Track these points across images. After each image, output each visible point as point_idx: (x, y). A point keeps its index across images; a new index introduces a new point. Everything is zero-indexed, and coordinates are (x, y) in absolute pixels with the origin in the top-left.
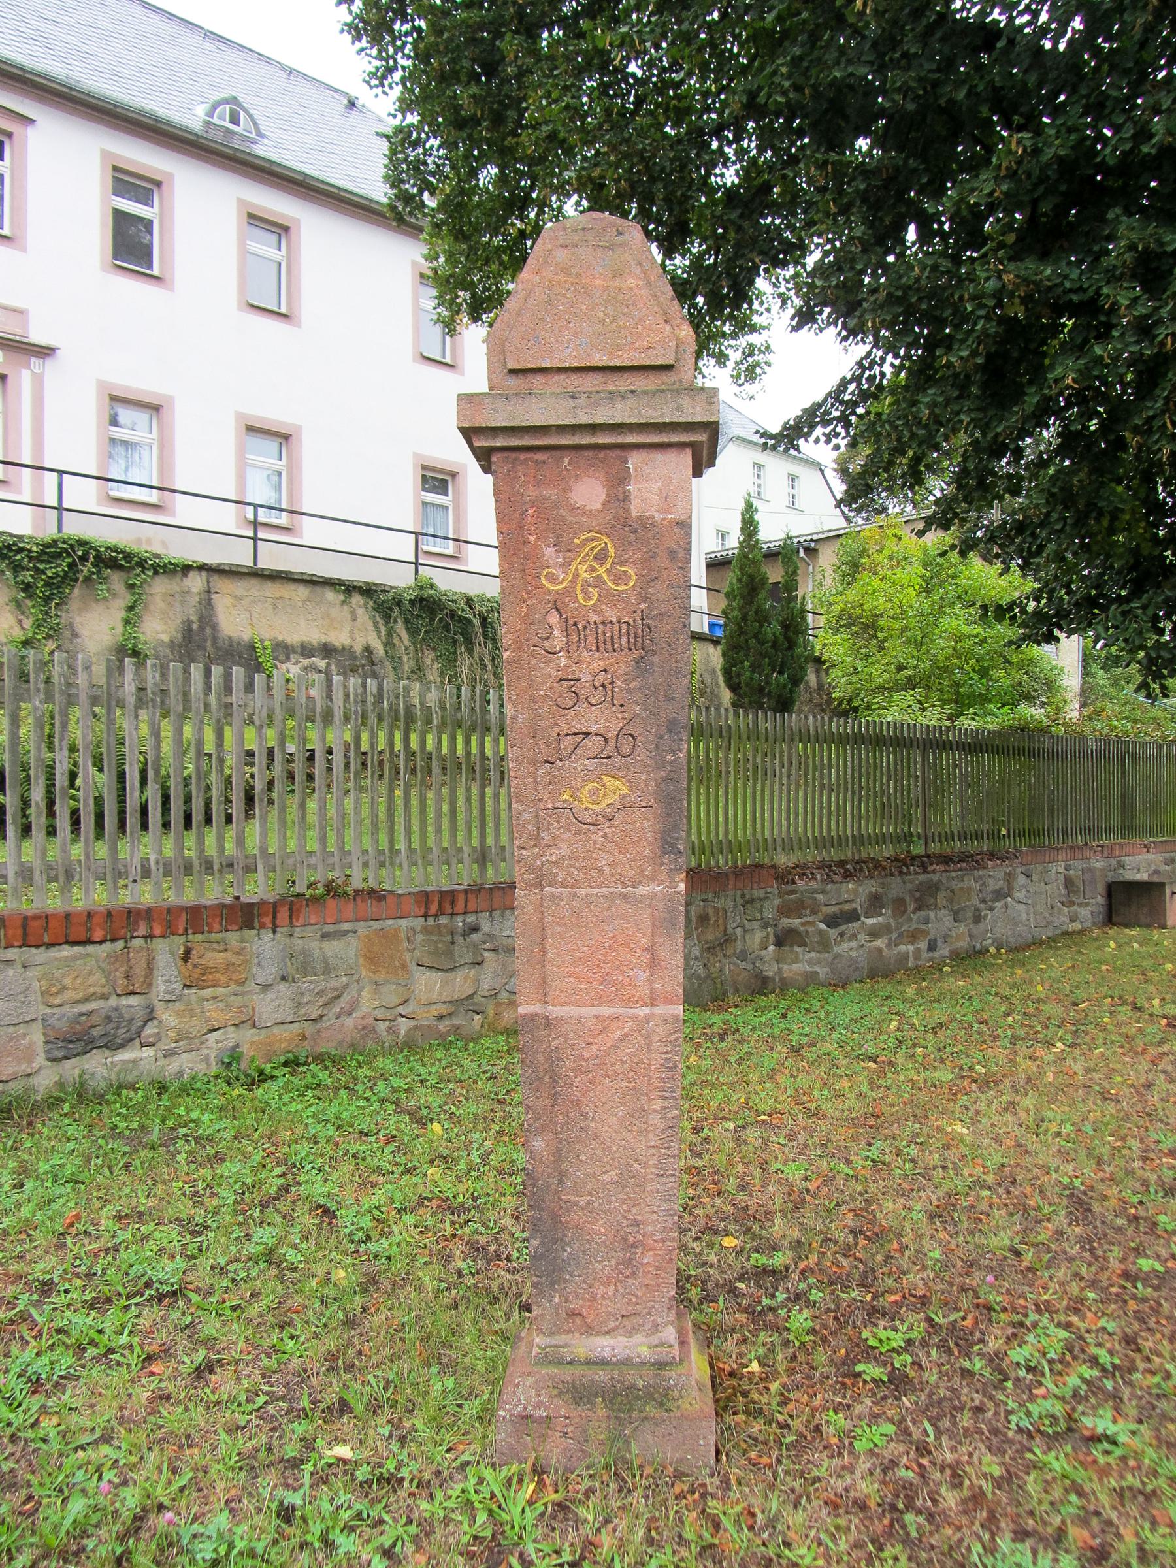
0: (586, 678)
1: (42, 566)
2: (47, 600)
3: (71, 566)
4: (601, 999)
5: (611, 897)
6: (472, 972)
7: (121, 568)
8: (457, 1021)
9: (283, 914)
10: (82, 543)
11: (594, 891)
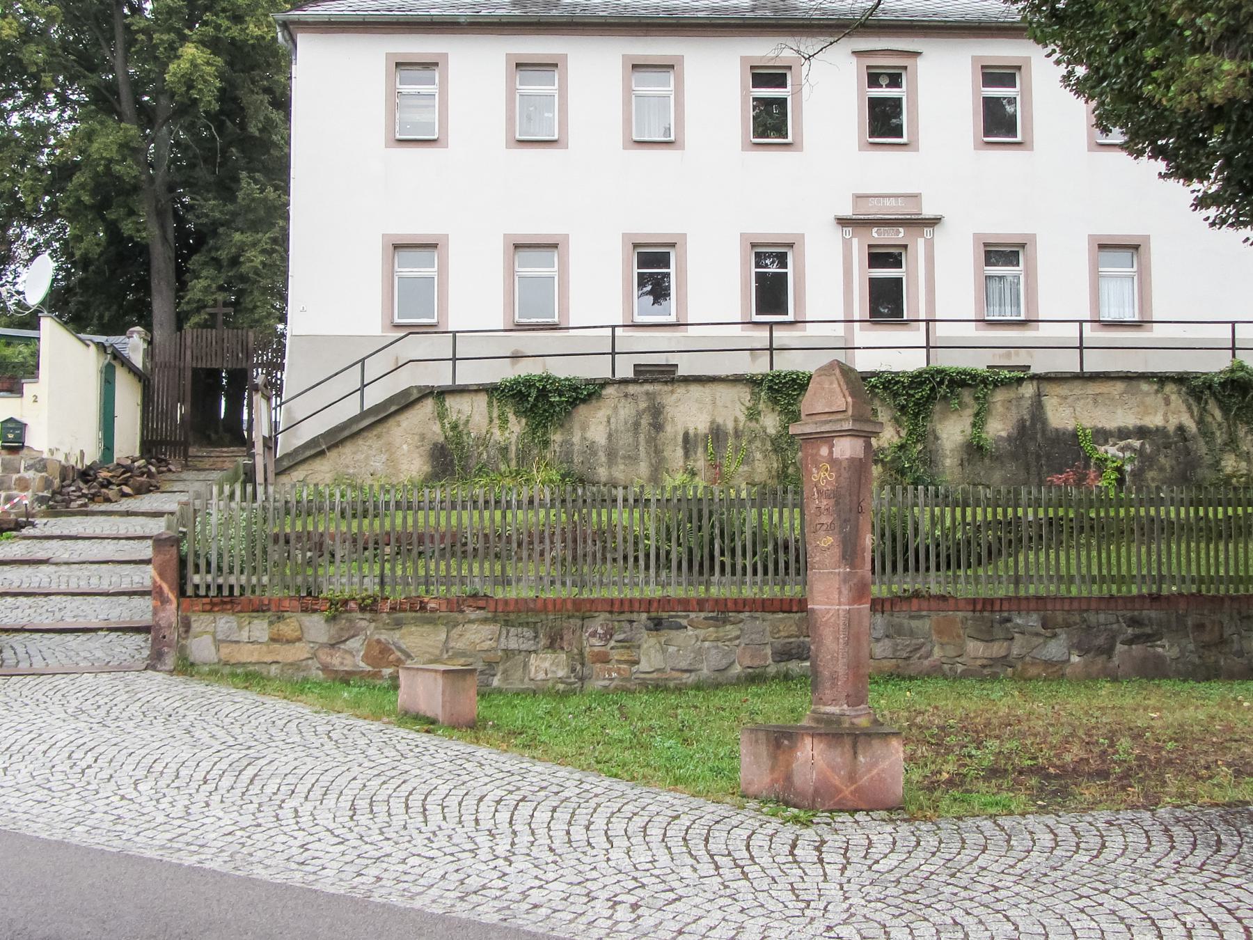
1: (911, 392)
2: (916, 415)
3: (932, 389)
7: (970, 385)
8: (995, 670)
9: (887, 606)
10: (939, 372)
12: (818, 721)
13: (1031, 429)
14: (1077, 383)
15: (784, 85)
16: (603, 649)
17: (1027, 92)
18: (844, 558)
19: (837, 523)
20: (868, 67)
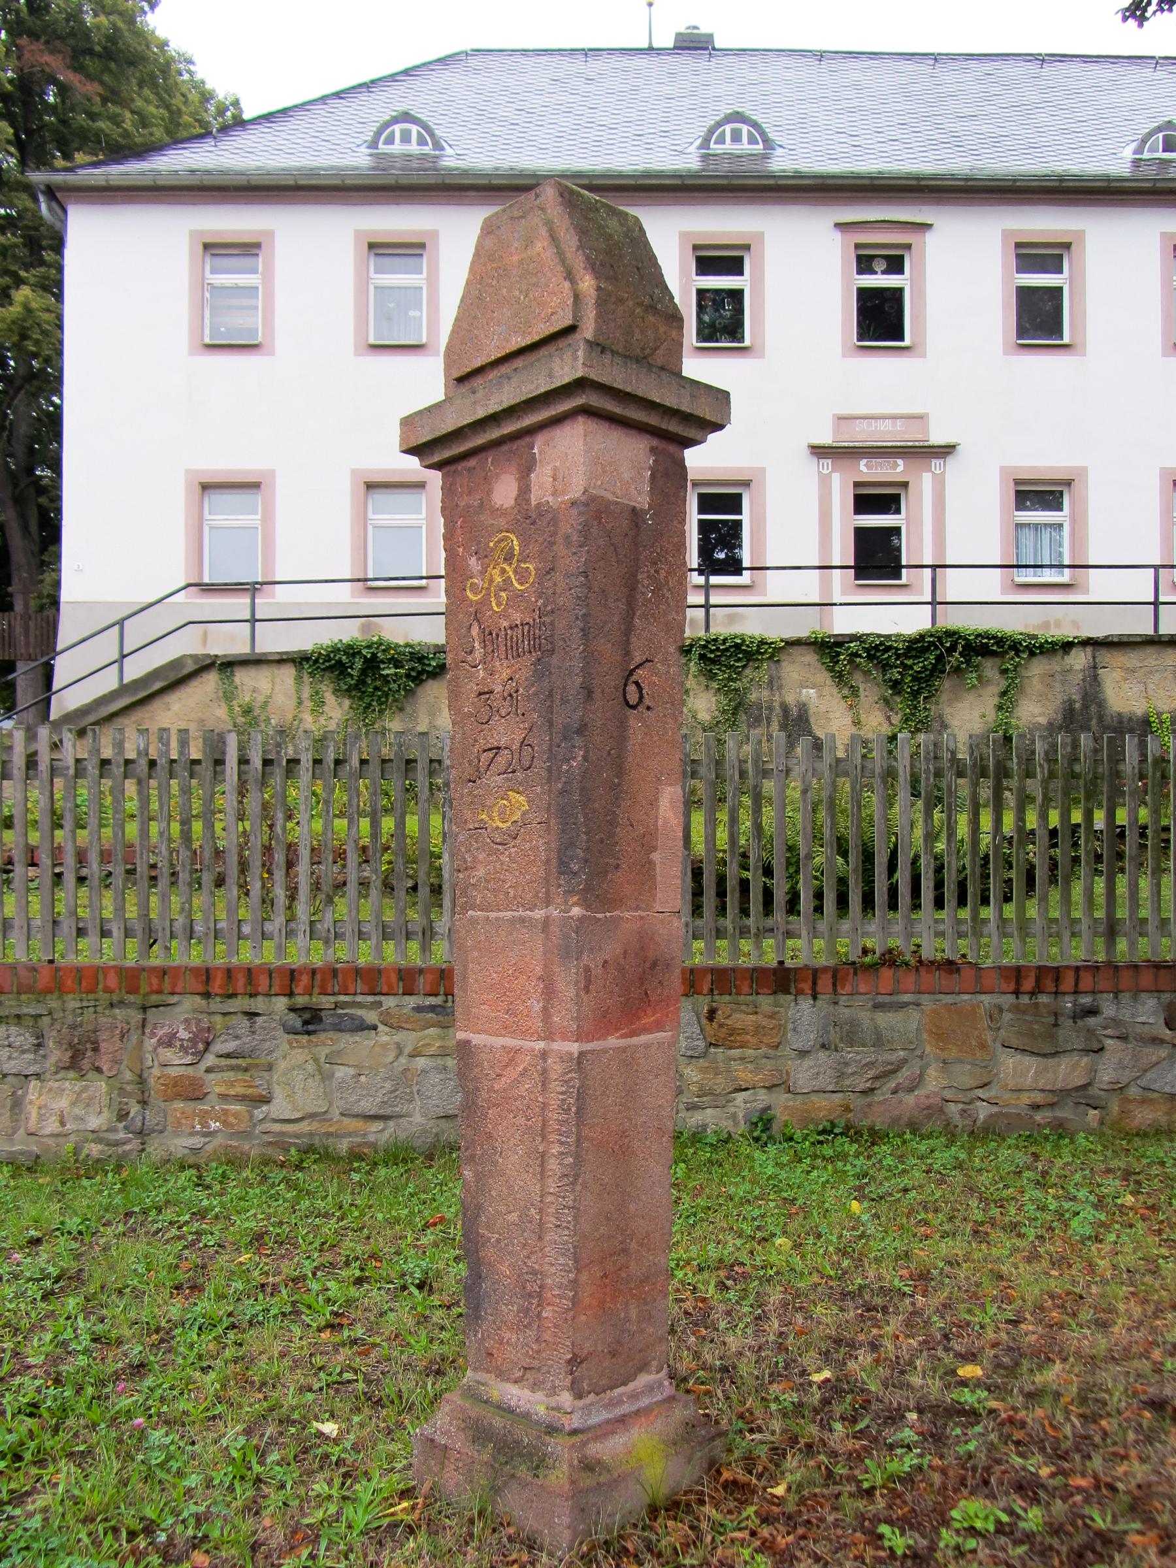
0: (498, 689)
1: (909, 662)
2: (915, 694)
3: (939, 658)
4: (506, 1030)
5: (512, 921)
6: (1085, 1060)
7: (994, 654)
8: (1060, 1113)
9: (825, 982)
10: (949, 634)
11: (501, 914)
12: (479, 1433)
13: (1083, 713)
14: (1150, 650)
15: (740, 272)
16: (190, 1071)
17: (1077, 280)
18: (563, 867)
19: (541, 741)
20: (858, 246)
